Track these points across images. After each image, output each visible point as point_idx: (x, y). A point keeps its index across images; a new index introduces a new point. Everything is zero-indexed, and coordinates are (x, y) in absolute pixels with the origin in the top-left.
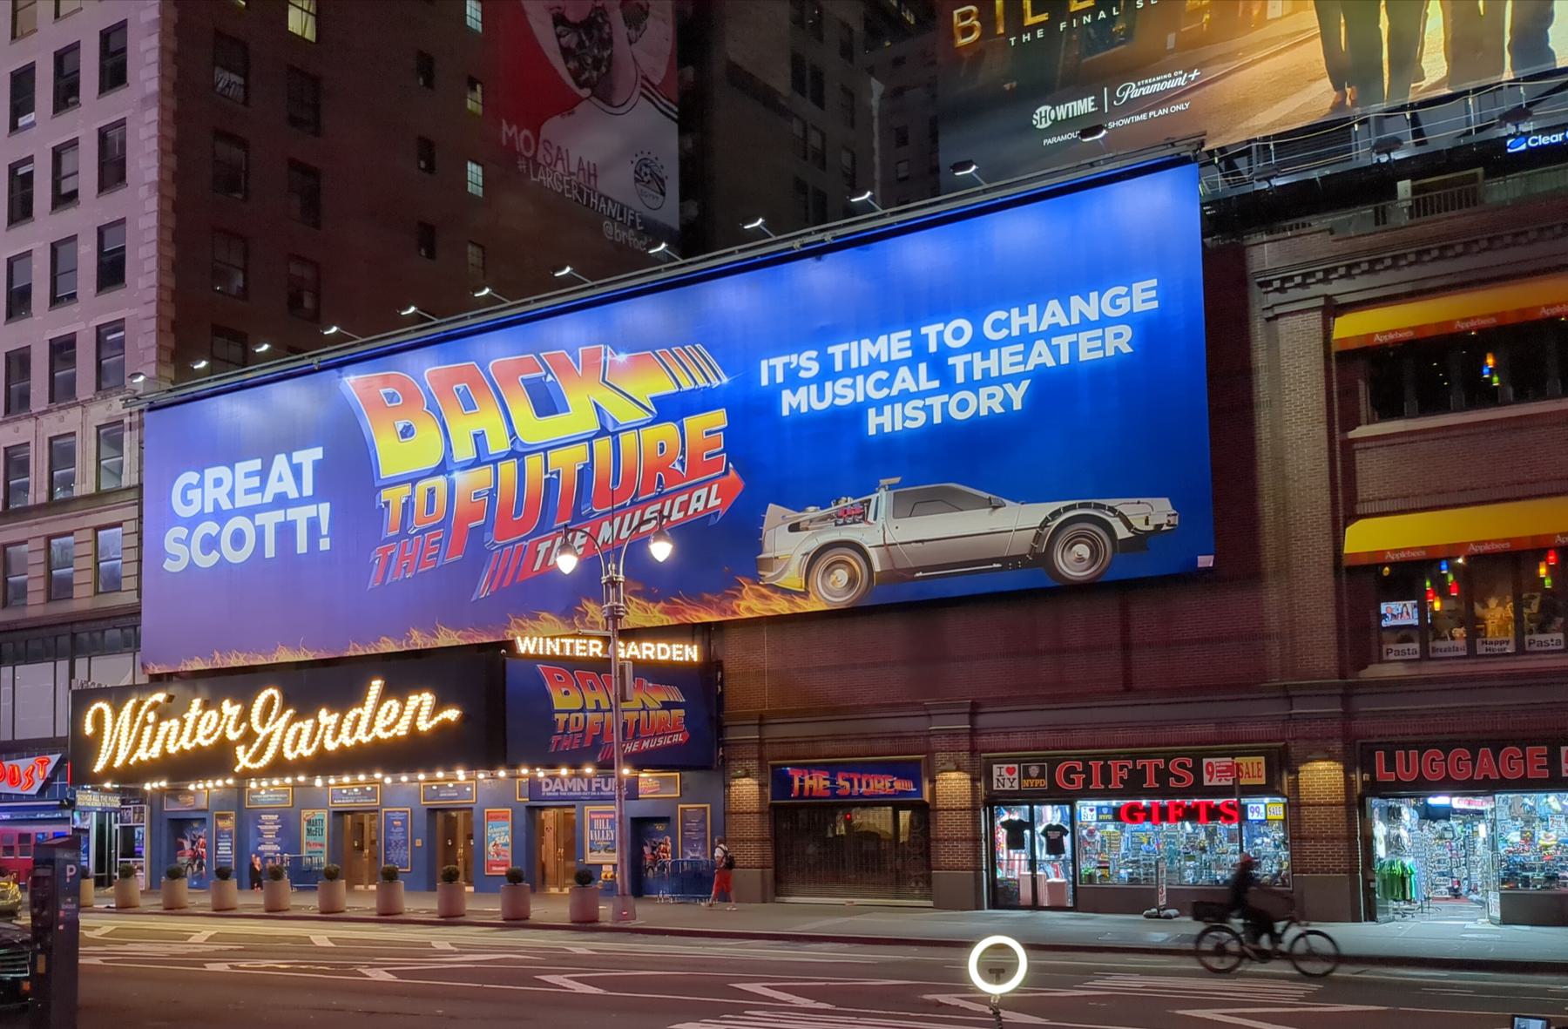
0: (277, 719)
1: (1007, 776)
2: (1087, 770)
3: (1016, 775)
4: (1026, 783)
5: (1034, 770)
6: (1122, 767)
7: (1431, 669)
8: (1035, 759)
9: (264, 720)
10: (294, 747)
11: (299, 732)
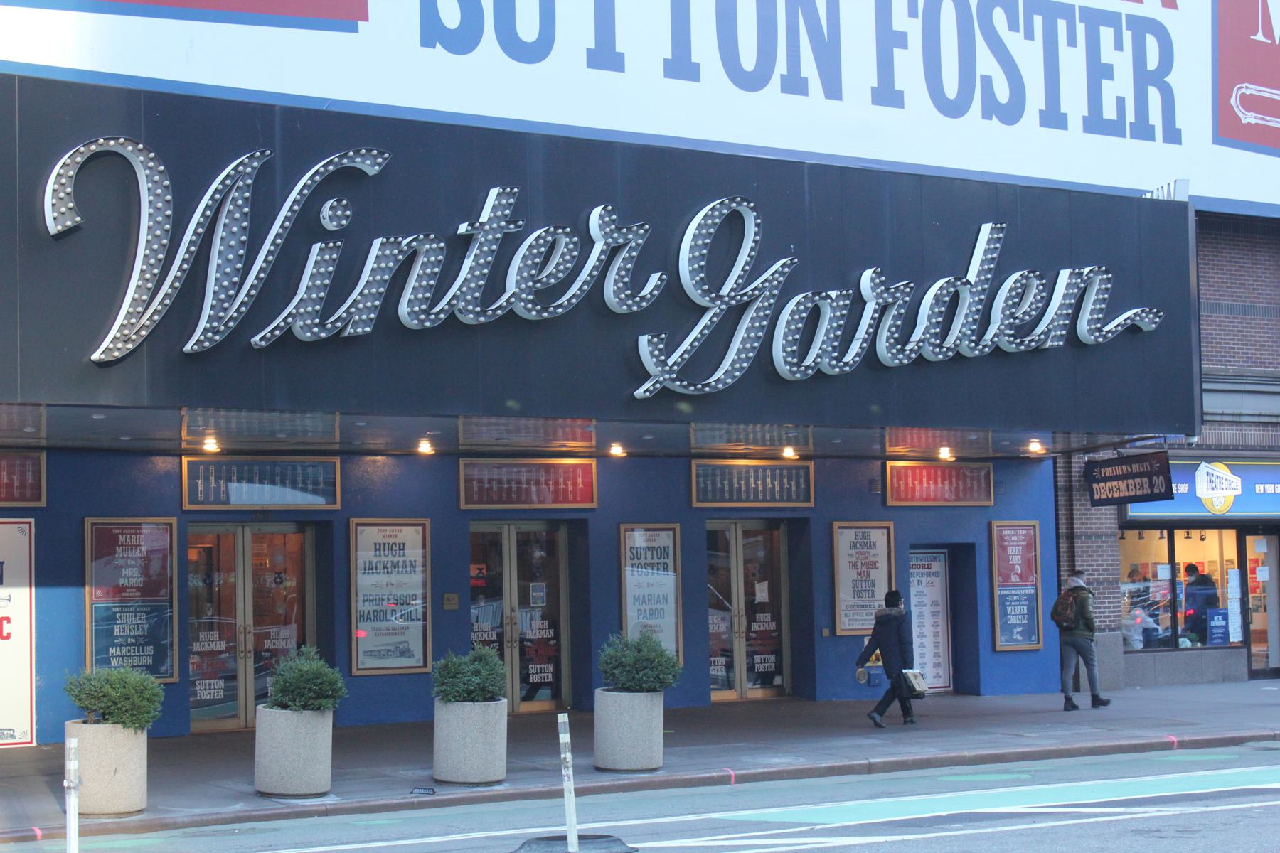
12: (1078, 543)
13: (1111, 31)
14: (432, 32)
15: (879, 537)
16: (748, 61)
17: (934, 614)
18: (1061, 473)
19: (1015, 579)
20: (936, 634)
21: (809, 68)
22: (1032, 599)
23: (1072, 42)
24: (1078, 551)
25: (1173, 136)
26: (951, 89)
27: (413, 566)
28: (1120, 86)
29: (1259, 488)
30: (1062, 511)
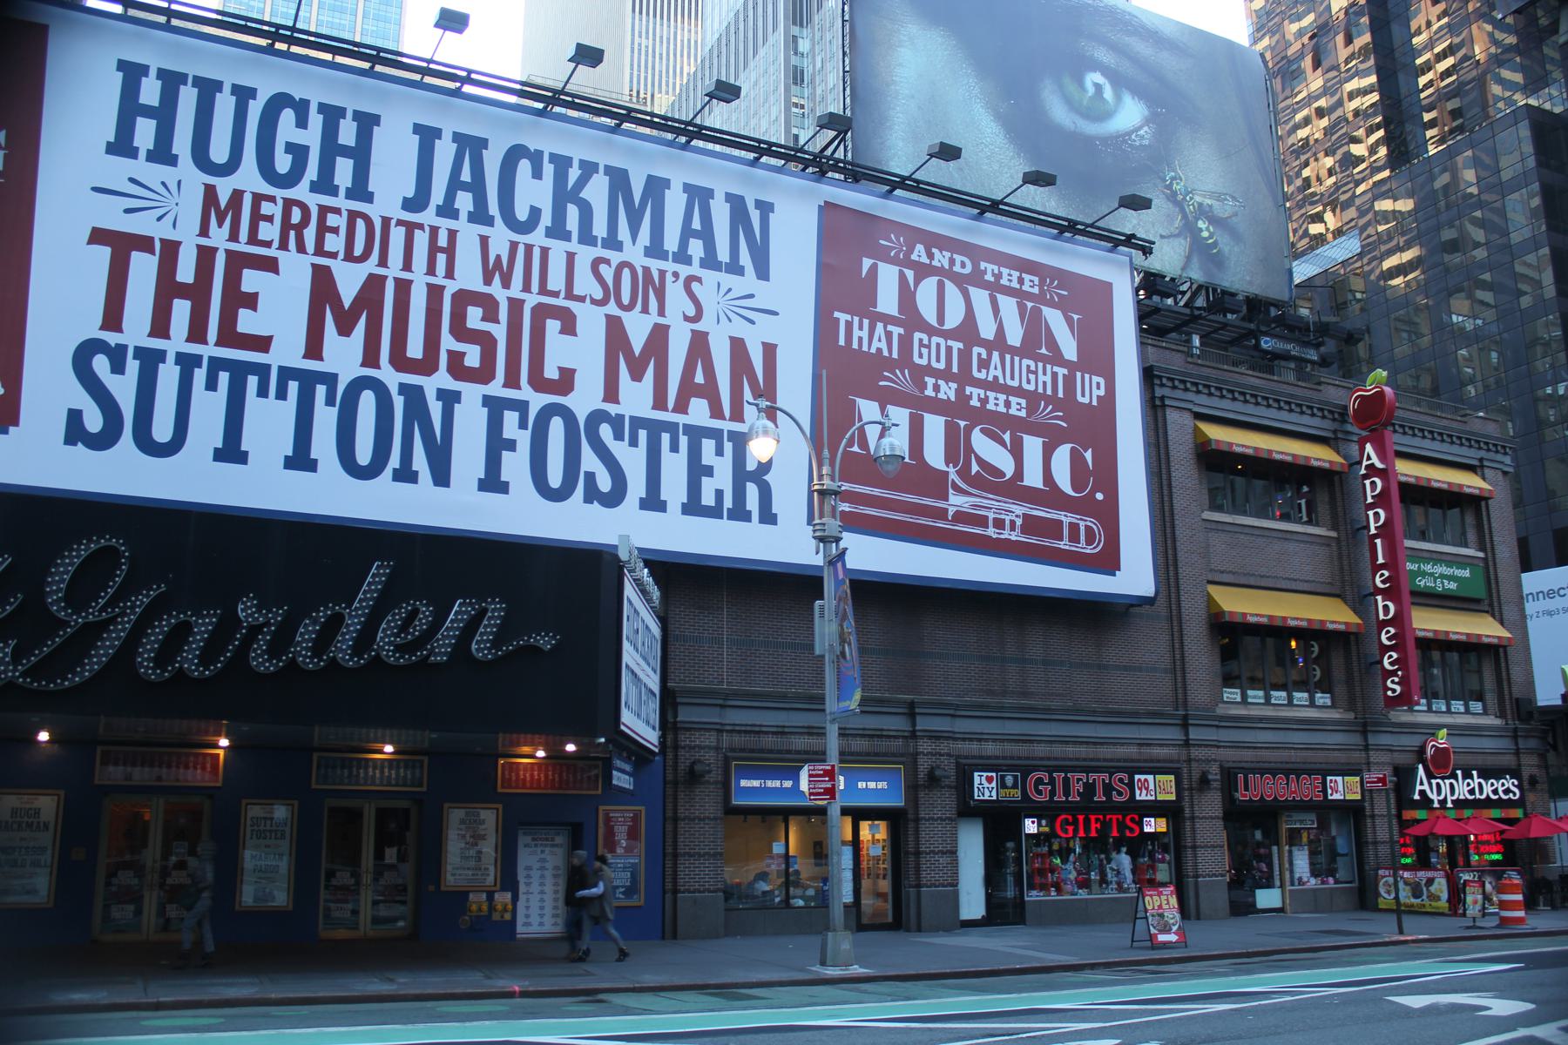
0: (122, 594)
1: (986, 785)
2: (1052, 782)
3: (994, 784)
4: (1002, 791)
5: (1009, 780)
7: (1269, 712)
8: (1011, 768)
9: (78, 595)
10: (162, 659)
11: (182, 632)
12: (681, 824)
13: (713, 442)
14: (75, 431)
15: (255, 811)
16: (364, 456)
17: (555, 876)
18: (670, 771)
19: (619, 851)
20: (556, 892)
21: (420, 462)
23: (674, 448)
24: (681, 831)
25: (768, 517)
26: (555, 479)
27: (46, 826)
28: (721, 478)
29: (862, 785)
30: (669, 800)
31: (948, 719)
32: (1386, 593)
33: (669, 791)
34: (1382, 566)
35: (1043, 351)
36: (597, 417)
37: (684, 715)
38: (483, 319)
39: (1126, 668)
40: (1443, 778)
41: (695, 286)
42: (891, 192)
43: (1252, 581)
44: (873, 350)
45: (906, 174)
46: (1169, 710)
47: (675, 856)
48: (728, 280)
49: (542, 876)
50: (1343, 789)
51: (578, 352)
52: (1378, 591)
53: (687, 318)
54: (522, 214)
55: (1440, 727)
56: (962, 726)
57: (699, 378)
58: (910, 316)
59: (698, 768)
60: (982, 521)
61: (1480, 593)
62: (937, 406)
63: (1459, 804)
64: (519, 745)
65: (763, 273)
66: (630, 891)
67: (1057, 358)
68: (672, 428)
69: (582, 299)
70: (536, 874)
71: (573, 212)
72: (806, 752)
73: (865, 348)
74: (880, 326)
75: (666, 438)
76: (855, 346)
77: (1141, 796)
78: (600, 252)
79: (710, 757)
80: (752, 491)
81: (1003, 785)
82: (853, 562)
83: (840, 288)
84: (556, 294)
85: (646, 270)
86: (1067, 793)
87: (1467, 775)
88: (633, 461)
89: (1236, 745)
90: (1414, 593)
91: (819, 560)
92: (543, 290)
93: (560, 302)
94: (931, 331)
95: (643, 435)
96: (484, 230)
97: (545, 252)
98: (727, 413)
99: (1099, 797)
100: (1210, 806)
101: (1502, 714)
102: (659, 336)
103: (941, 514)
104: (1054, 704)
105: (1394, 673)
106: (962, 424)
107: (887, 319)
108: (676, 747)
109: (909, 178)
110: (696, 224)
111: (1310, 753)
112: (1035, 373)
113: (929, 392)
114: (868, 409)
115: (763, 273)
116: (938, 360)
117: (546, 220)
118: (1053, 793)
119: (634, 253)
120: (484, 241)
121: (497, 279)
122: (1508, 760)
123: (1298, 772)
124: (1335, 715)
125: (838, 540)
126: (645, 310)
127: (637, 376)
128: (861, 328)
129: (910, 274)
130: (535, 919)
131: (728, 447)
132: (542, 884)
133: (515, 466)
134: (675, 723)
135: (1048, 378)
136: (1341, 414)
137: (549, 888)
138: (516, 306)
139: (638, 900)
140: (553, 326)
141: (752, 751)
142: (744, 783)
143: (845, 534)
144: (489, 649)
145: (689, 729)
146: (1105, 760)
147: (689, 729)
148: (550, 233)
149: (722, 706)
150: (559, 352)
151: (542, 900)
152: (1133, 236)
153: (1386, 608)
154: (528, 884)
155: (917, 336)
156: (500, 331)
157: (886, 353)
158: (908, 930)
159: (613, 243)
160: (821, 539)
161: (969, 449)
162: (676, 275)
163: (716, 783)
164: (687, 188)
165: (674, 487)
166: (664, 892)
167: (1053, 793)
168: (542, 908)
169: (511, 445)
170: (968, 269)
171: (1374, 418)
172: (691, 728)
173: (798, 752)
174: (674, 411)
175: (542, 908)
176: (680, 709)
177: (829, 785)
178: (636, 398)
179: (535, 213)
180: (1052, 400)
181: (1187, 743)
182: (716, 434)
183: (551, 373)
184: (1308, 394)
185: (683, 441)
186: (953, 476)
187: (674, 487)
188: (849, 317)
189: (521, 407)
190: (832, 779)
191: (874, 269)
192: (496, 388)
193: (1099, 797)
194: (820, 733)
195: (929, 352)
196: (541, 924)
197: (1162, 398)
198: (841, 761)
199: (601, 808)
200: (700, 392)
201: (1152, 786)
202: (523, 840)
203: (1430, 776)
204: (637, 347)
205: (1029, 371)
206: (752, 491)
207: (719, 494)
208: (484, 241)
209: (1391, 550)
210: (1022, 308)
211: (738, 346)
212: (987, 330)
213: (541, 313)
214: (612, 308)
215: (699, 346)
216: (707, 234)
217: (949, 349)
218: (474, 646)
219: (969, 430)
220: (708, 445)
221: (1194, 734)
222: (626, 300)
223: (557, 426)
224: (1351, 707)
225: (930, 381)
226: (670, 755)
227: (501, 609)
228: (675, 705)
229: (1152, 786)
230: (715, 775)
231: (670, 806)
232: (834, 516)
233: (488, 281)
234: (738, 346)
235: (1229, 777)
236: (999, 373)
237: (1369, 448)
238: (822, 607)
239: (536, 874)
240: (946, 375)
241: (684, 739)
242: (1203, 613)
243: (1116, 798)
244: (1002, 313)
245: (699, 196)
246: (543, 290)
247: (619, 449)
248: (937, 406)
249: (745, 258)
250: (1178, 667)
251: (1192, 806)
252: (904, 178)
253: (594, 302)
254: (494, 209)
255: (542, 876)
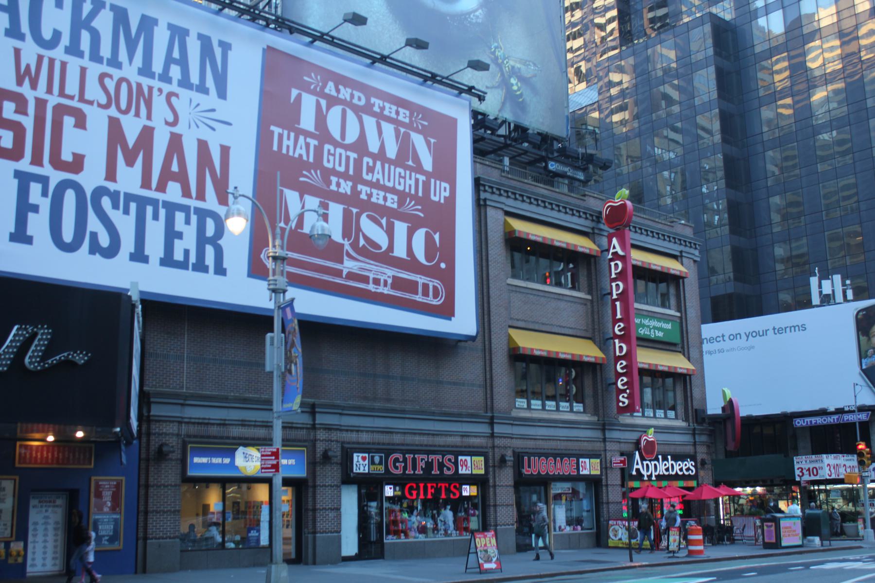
4: (372, 467)
5: (377, 459)
6: (422, 460)
8: (378, 451)
12: (151, 490)
17: (55, 529)
18: (143, 450)
19: (106, 509)
20: (56, 541)
22: (116, 521)
23: (156, 217)
24: (150, 494)
25: (220, 270)
26: (68, 235)
28: (188, 242)
30: (143, 472)
31: (337, 416)
32: (622, 338)
33: (143, 466)
34: (620, 320)
35: (410, 163)
36: (100, 192)
37: (156, 411)
38: (16, 112)
39: (455, 384)
40: (650, 461)
41: (174, 100)
42: (312, 42)
43: (536, 327)
44: (296, 155)
45: (325, 31)
46: (482, 413)
47: (146, 513)
48: (197, 97)
49: (46, 529)
50: (590, 467)
51: (87, 141)
52: (616, 336)
53: (167, 123)
54: (47, 35)
55: (649, 427)
56: (347, 421)
57: (175, 168)
58: (322, 134)
59: (165, 449)
60: (365, 279)
61: (677, 339)
62: (339, 198)
63: (660, 478)
64: (32, 432)
65: (222, 94)
66: (113, 539)
67: (419, 169)
68: (154, 203)
69: (91, 103)
70: (41, 528)
71: (85, 38)
72: (240, 438)
73: (291, 154)
74: (302, 138)
75: (149, 210)
76: (284, 151)
77: (462, 471)
78: (105, 68)
79: (173, 442)
80: (210, 251)
81: (372, 462)
82: (299, 308)
83: (275, 109)
84: (72, 98)
85: (139, 86)
86: (414, 469)
87: (665, 459)
88: (126, 225)
89: (523, 437)
90: (639, 339)
91: (271, 305)
92: (62, 94)
93: (75, 103)
94: (336, 144)
95: (133, 206)
96: (18, 44)
97: (64, 65)
98: (194, 194)
99: (435, 472)
100: (506, 478)
101: (686, 420)
102: (147, 134)
103: (338, 273)
104: (408, 407)
105: (624, 391)
106: (355, 211)
107: (307, 134)
108: (149, 434)
109: (327, 34)
110: (176, 54)
111: (569, 444)
112: (404, 178)
113: (333, 187)
114: (292, 197)
115: (222, 94)
116: (340, 165)
117: (65, 41)
118: (405, 468)
119: (130, 71)
120: (17, 52)
121: (27, 82)
122: (689, 449)
123: (562, 456)
124: (586, 418)
125: (284, 291)
126: (137, 114)
127: (130, 163)
128: (289, 139)
129: (323, 103)
130: (39, 561)
131: (194, 218)
132: (45, 535)
133: (38, 224)
134: (149, 416)
135: (413, 182)
136: (597, 218)
137: (50, 537)
138: (41, 104)
139: (117, 546)
140: (69, 121)
141: (202, 437)
142: (197, 460)
143: (289, 289)
144: (39, 362)
145: (159, 421)
146: (440, 446)
147: (159, 421)
148: (68, 51)
149: (182, 405)
150: (73, 141)
151: (45, 547)
152: (473, 87)
153: (621, 348)
154: (35, 536)
155: (327, 147)
156: (28, 122)
157: (305, 158)
158: (306, 564)
159: (114, 62)
160: (274, 291)
161: (359, 229)
162: (160, 90)
163: (177, 460)
164: (171, 27)
165: (155, 246)
166: (137, 540)
167: (405, 468)
168: (45, 553)
169: (35, 209)
170: (363, 102)
171: (618, 220)
172: (160, 420)
173: (234, 438)
174: (157, 190)
175: (45, 553)
176: (153, 407)
177: (275, 462)
178: (129, 179)
179: (57, 35)
180: (415, 197)
181: (492, 435)
182: (186, 209)
183: (66, 156)
184: (578, 202)
185: (162, 212)
186: (347, 247)
187: (155, 246)
188: (280, 130)
189: (44, 180)
190: (277, 458)
191: (299, 97)
192: (25, 165)
193: (435, 472)
194: (268, 426)
195: (335, 159)
196: (44, 565)
197: (485, 200)
198: (283, 446)
199: (93, 478)
200: (175, 177)
201: (469, 465)
202: (33, 502)
203: (643, 459)
204: (131, 141)
205: (400, 176)
206: (210, 251)
207: (187, 252)
208: (17, 52)
209: (626, 310)
210: (397, 132)
211: (203, 146)
212: (373, 146)
213: (61, 111)
214: (113, 112)
215: (175, 144)
216: (183, 62)
217: (348, 158)
218: (27, 360)
219: (358, 216)
220: (180, 216)
221: (497, 429)
222: (123, 106)
223: (70, 197)
224: (596, 412)
225: (334, 179)
226: (144, 440)
227: (48, 333)
228: (149, 404)
229: (469, 465)
230: (177, 455)
231: (143, 477)
232: (282, 274)
233: (20, 83)
234: (203, 146)
235: (519, 458)
236: (380, 177)
237: (615, 241)
238: (272, 338)
239: (41, 528)
240: (345, 176)
241: (155, 428)
242: (505, 348)
243: (446, 472)
244: (384, 135)
245: (178, 34)
246: (62, 94)
247: (116, 216)
248: (339, 198)
249: (210, 83)
250: (488, 384)
251: (494, 477)
252: (323, 34)
253: (100, 105)
254: (25, 27)
255: (46, 529)
